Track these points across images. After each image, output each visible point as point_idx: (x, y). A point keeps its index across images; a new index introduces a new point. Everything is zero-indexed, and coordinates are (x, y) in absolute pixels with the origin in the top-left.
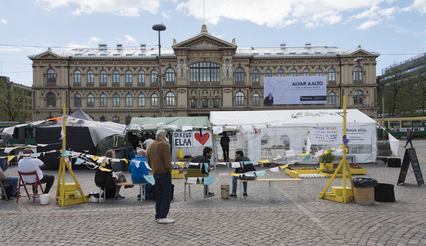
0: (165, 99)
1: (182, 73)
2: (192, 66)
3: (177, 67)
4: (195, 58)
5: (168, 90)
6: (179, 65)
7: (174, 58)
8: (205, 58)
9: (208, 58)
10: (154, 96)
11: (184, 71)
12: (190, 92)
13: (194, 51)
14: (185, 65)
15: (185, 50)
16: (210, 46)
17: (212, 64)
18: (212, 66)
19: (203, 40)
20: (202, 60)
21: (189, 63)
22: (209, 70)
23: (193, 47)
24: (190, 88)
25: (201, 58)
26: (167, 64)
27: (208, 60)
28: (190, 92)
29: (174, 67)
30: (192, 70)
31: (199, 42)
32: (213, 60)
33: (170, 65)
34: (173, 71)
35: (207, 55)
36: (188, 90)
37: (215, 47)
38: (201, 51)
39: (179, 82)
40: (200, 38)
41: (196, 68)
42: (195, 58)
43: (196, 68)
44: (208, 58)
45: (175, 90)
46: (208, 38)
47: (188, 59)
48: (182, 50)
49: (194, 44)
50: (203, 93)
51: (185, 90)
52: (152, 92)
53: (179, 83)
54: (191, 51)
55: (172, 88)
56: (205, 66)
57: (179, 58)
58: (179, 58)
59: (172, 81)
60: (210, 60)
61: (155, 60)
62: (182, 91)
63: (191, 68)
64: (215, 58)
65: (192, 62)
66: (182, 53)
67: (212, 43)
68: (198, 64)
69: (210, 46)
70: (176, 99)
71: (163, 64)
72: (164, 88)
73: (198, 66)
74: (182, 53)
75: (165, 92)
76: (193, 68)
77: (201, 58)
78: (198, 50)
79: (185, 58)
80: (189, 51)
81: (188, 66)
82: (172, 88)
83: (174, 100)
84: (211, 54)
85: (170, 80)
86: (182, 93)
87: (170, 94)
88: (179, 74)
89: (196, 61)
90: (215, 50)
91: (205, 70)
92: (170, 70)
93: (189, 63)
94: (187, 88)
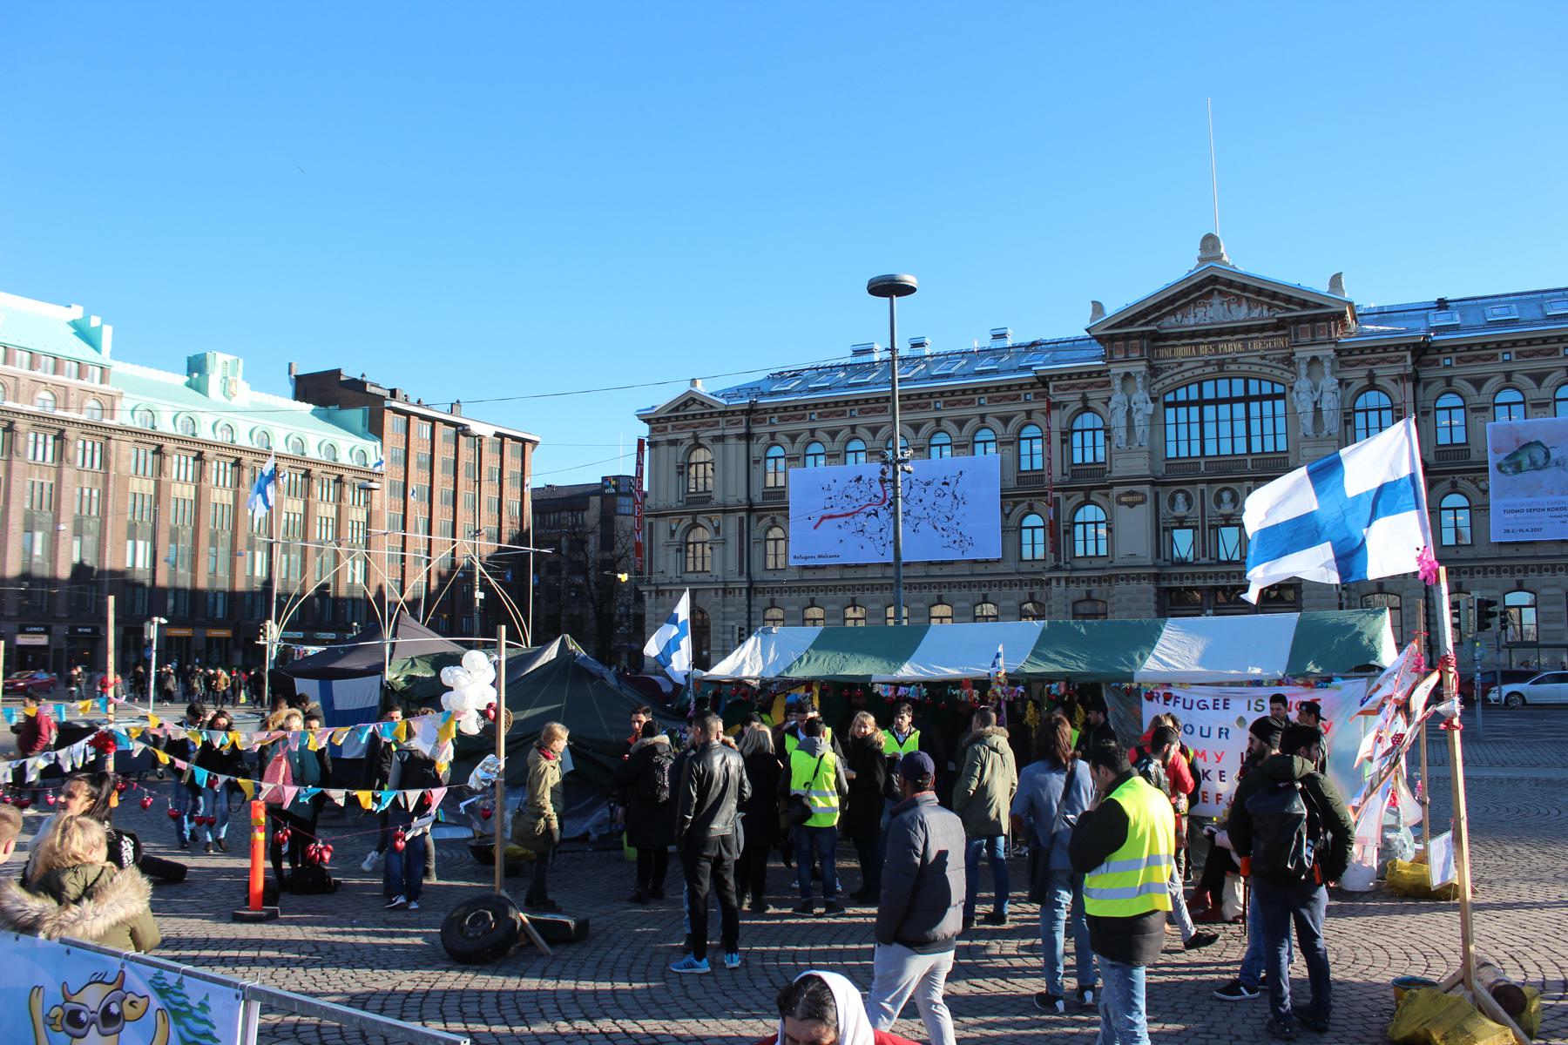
0: (1070, 531)
1: (1130, 427)
2: (1170, 398)
3: (1112, 405)
4: (1180, 364)
5: (1080, 496)
6: (1118, 398)
7: (1099, 373)
8: (1221, 364)
9: (1235, 361)
10: (1033, 520)
11: (1138, 418)
12: (1164, 502)
13: (1180, 336)
14: (1140, 396)
15: (1141, 336)
16: (1241, 314)
17: (1253, 384)
18: (1254, 391)
19: (1210, 293)
20: (1209, 369)
21: (1159, 386)
22: (1239, 409)
23: (1170, 324)
24: (1164, 484)
25: (1207, 363)
26: (1073, 398)
27: (1234, 367)
28: (1164, 502)
29: (1100, 407)
30: (1170, 412)
31: (1194, 301)
32: (1255, 368)
33: (1085, 399)
34: (1099, 424)
35: (1231, 348)
36: (1157, 494)
37: (1261, 314)
38: (1207, 333)
39: (1119, 463)
40: (1198, 287)
41: (1188, 404)
42: (1180, 364)
43: (1188, 404)
44: (1235, 361)
45: (1107, 495)
46: (1230, 284)
47: (1154, 371)
48: (1128, 337)
49: (1172, 313)
50: (1219, 501)
51: (1143, 494)
52: (1024, 507)
53: (1123, 466)
54: (1167, 337)
55: (1093, 488)
56: (1224, 393)
57: (1117, 370)
58: (1117, 370)
59: (1095, 462)
60: (1244, 367)
61: (1032, 385)
62: (1130, 499)
63: (1168, 405)
64: (1263, 357)
65: (1167, 382)
66: (1126, 351)
67: (1248, 299)
68: (1194, 389)
69: (1241, 314)
70: (1109, 530)
71: (1058, 399)
72: (1064, 490)
73: (1194, 395)
74: (1126, 351)
75: (1066, 507)
76: (1176, 404)
77: (1207, 363)
78: (1193, 335)
79: (1140, 368)
80: (1156, 337)
81: (1154, 400)
82: (1093, 488)
83: (1102, 531)
84: (1245, 346)
85: (1089, 459)
86: (1131, 505)
87: (1090, 513)
88: (1120, 433)
89: (1187, 375)
90: (1262, 328)
91: (1224, 410)
92: (1087, 420)
93: (1159, 386)
94: (1153, 484)
